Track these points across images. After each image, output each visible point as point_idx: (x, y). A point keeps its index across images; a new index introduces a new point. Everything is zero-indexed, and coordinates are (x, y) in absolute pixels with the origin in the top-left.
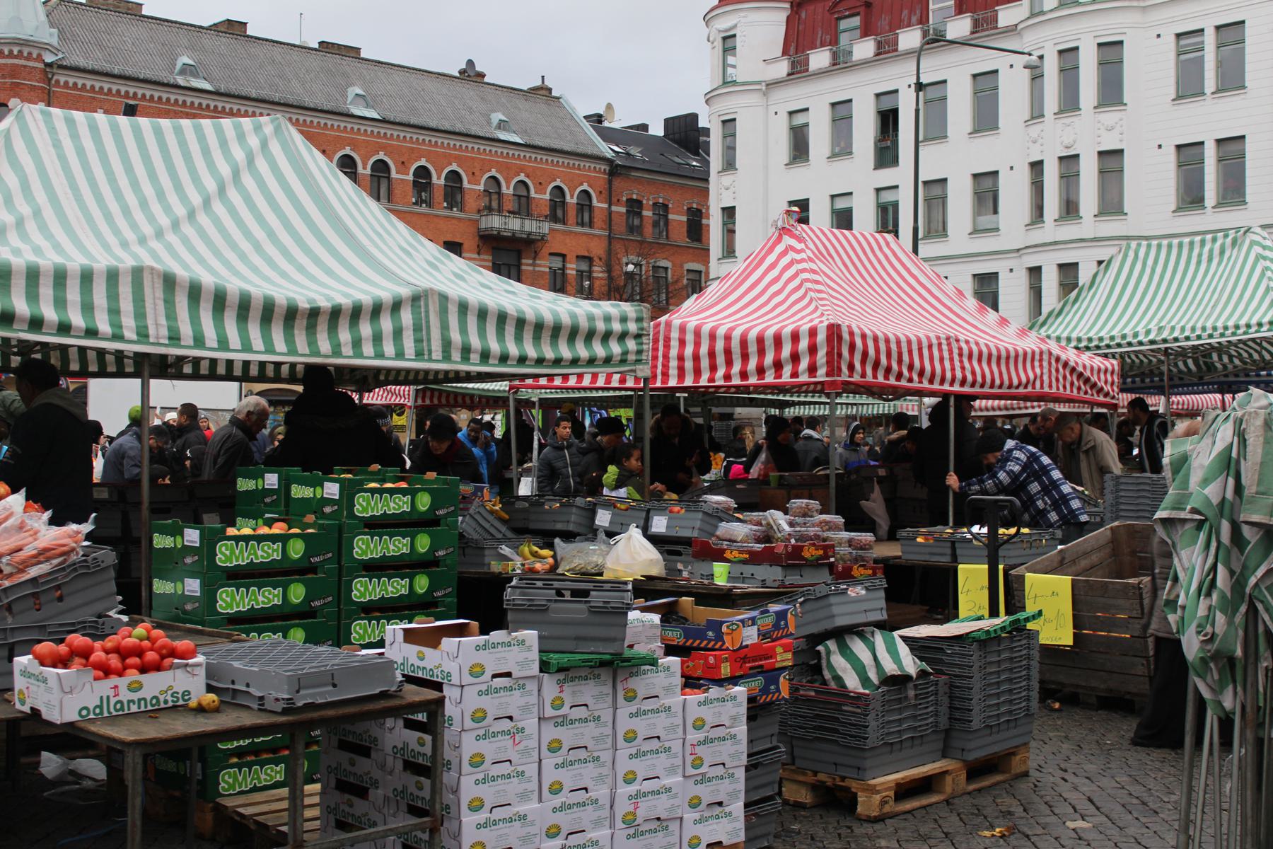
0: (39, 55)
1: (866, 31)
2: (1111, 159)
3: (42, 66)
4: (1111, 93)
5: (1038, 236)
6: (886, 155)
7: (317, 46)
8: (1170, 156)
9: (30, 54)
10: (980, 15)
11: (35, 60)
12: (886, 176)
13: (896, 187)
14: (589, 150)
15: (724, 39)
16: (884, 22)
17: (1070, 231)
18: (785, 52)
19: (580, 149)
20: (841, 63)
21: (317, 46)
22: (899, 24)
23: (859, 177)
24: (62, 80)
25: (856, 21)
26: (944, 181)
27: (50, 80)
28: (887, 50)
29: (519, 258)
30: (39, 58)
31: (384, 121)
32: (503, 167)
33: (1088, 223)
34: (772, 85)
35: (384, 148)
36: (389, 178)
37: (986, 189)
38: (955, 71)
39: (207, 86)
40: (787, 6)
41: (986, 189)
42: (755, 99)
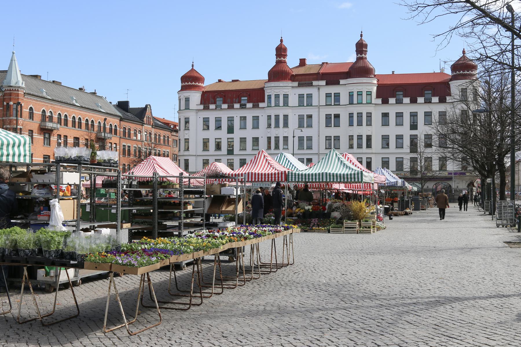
1: (224, 103)
10: (255, 104)
12: (230, 136)
16: (229, 100)
18: (201, 104)
23: (223, 134)
26: (246, 138)
28: (231, 107)
41: (256, 140)
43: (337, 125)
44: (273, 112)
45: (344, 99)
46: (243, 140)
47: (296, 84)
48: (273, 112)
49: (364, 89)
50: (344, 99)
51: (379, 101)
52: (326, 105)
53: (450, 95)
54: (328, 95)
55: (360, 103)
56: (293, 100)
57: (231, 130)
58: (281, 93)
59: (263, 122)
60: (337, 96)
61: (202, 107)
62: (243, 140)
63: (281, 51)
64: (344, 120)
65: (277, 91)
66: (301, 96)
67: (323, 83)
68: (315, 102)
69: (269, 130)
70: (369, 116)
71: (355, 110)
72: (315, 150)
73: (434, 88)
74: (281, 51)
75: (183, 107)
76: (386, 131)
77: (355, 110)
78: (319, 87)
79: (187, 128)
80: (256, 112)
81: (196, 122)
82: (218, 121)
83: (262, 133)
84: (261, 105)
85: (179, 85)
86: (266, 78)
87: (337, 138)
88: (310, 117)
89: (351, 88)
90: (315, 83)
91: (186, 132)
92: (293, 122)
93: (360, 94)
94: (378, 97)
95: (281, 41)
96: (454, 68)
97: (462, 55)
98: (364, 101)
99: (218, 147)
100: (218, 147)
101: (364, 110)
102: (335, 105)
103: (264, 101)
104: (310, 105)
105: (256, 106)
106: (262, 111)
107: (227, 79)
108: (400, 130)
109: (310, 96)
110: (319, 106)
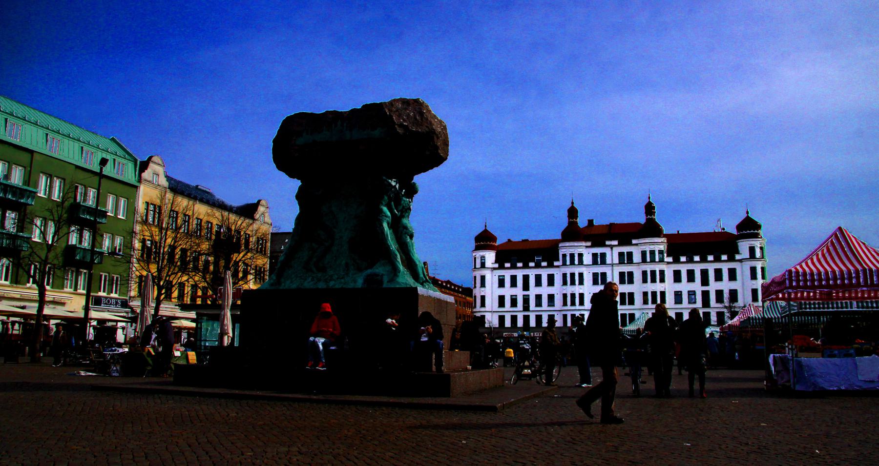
5: (565, 308)
6: (526, 287)
12: (526, 293)
17: (573, 308)
18: (496, 262)
23: (519, 292)
34: (495, 269)
37: (551, 298)
38: (544, 273)
43: (631, 281)
44: (568, 270)
45: (637, 258)
47: (589, 244)
48: (568, 270)
49: (657, 248)
50: (637, 258)
51: (670, 259)
53: (738, 253)
54: (621, 255)
55: (653, 261)
56: (587, 259)
57: (526, 287)
58: (576, 251)
59: (558, 280)
60: (630, 254)
61: (497, 265)
63: (573, 212)
64: (638, 277)
65: (572, 251)
66: (595, 256)
67: (616, 243)
68: (608, 261)
69: (564, 287)
70: (662, 273)
71: (649, 268)
73: (720, 245)
74: (573, 212)
75: (478, 265)
76: (678, 287)
77: (649, 268)
78: (612, 247)
79: (483, 285)
80: (551, 271)
81: (492, 279)
82: (514, 279)
83: (557, 290)
84: (556, 263)
85: (473, 244)
86: (560, 237)
87: (631, 295)
89: (644, 248)
90: (607, 243)
91: (483, 289)
93: (652, 253)
94: (668, 256)
95: (573, 203)
96: (739, 227)
97: (745, 215)
98: (657, 260)
99: (514, 302)
100: (514, 302)
101: (657, 268)
103: (558, 260)
104: (603, 262)
105: (551, 265)
106: (532, 270)
107: (516, 238)
108: (692, 286)
109: (603, 255)
110: (612, 265)
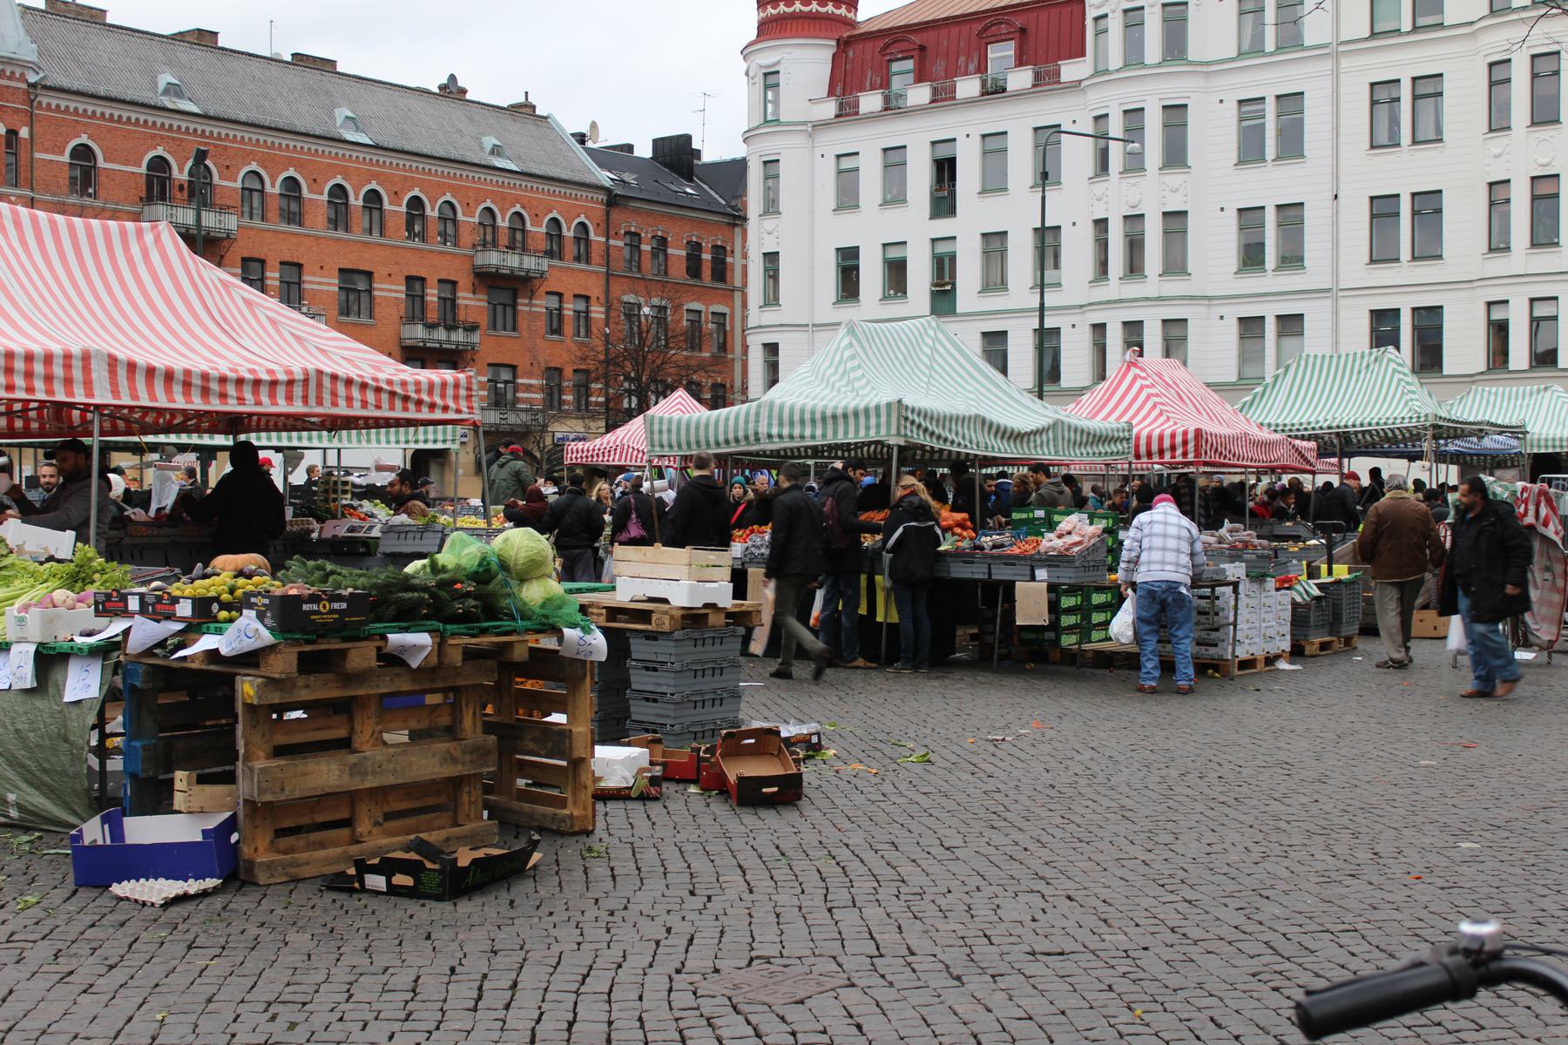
0: (22, 75)
1: (920, 77)
2: (1175, 220)
3: (24, 86)
4: (1175, 156)
6: (944, 204)
7: (289, 59)
8: (1232, 219)
9: (13, 73)
10: (1043, 68)
11: (18, 80)
12: (943, 227)
13: (954, 238)
14: (588, 179)
15: (766, 75)
16: (939, 67)
17: (1134, 289)
18: (831, 93)
19: (577, 178)
20: (892, 107)
21: (289, 59)
22: (954, 72)
23: (914, 227)
24: (45, 101)
25: (909, 64)
27: (32, 101)
28: (943, 97)
29: (515, 297)
30: (23, 78)
31: (377, 147)
32: (501, 198)
33: (1153, 282)
34: (820, 126)
35: (376, 176)
36: (381, 209)
38: (1018, 122)
39: (195, 109)
40: (834, 43)
41: (1047, 240)
42: (800, 140)
46: (995, 242)
52: (1374, 35)
62: (995, 242)
72: (1316, 269)
80: (1049, 110)
83: (1077, 202)
84: (1071, 70)
88: (1291, 102)
92: (1213, 132)
102: (1416, 29)
105: (1046, 80)
110: (1336, 50)
